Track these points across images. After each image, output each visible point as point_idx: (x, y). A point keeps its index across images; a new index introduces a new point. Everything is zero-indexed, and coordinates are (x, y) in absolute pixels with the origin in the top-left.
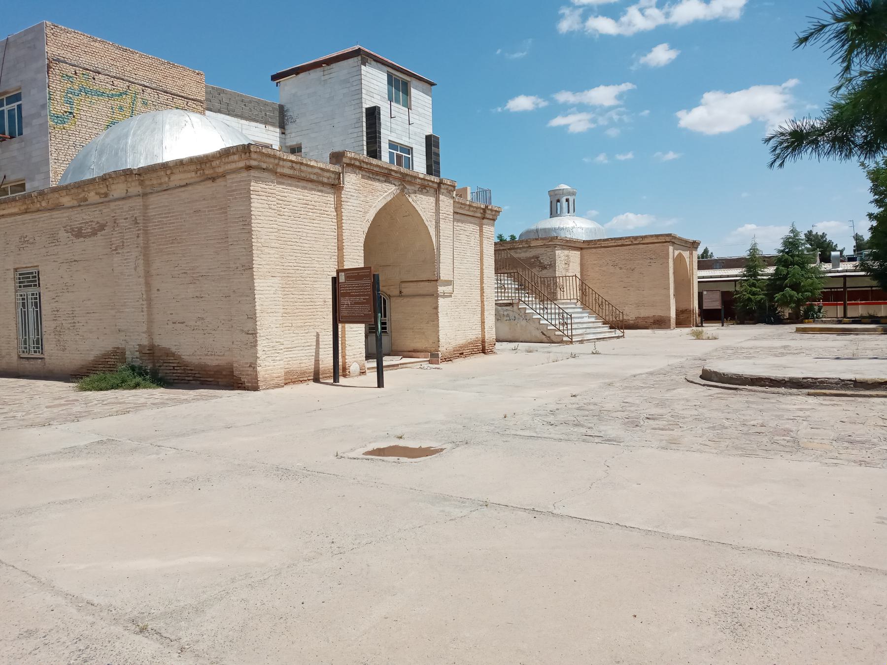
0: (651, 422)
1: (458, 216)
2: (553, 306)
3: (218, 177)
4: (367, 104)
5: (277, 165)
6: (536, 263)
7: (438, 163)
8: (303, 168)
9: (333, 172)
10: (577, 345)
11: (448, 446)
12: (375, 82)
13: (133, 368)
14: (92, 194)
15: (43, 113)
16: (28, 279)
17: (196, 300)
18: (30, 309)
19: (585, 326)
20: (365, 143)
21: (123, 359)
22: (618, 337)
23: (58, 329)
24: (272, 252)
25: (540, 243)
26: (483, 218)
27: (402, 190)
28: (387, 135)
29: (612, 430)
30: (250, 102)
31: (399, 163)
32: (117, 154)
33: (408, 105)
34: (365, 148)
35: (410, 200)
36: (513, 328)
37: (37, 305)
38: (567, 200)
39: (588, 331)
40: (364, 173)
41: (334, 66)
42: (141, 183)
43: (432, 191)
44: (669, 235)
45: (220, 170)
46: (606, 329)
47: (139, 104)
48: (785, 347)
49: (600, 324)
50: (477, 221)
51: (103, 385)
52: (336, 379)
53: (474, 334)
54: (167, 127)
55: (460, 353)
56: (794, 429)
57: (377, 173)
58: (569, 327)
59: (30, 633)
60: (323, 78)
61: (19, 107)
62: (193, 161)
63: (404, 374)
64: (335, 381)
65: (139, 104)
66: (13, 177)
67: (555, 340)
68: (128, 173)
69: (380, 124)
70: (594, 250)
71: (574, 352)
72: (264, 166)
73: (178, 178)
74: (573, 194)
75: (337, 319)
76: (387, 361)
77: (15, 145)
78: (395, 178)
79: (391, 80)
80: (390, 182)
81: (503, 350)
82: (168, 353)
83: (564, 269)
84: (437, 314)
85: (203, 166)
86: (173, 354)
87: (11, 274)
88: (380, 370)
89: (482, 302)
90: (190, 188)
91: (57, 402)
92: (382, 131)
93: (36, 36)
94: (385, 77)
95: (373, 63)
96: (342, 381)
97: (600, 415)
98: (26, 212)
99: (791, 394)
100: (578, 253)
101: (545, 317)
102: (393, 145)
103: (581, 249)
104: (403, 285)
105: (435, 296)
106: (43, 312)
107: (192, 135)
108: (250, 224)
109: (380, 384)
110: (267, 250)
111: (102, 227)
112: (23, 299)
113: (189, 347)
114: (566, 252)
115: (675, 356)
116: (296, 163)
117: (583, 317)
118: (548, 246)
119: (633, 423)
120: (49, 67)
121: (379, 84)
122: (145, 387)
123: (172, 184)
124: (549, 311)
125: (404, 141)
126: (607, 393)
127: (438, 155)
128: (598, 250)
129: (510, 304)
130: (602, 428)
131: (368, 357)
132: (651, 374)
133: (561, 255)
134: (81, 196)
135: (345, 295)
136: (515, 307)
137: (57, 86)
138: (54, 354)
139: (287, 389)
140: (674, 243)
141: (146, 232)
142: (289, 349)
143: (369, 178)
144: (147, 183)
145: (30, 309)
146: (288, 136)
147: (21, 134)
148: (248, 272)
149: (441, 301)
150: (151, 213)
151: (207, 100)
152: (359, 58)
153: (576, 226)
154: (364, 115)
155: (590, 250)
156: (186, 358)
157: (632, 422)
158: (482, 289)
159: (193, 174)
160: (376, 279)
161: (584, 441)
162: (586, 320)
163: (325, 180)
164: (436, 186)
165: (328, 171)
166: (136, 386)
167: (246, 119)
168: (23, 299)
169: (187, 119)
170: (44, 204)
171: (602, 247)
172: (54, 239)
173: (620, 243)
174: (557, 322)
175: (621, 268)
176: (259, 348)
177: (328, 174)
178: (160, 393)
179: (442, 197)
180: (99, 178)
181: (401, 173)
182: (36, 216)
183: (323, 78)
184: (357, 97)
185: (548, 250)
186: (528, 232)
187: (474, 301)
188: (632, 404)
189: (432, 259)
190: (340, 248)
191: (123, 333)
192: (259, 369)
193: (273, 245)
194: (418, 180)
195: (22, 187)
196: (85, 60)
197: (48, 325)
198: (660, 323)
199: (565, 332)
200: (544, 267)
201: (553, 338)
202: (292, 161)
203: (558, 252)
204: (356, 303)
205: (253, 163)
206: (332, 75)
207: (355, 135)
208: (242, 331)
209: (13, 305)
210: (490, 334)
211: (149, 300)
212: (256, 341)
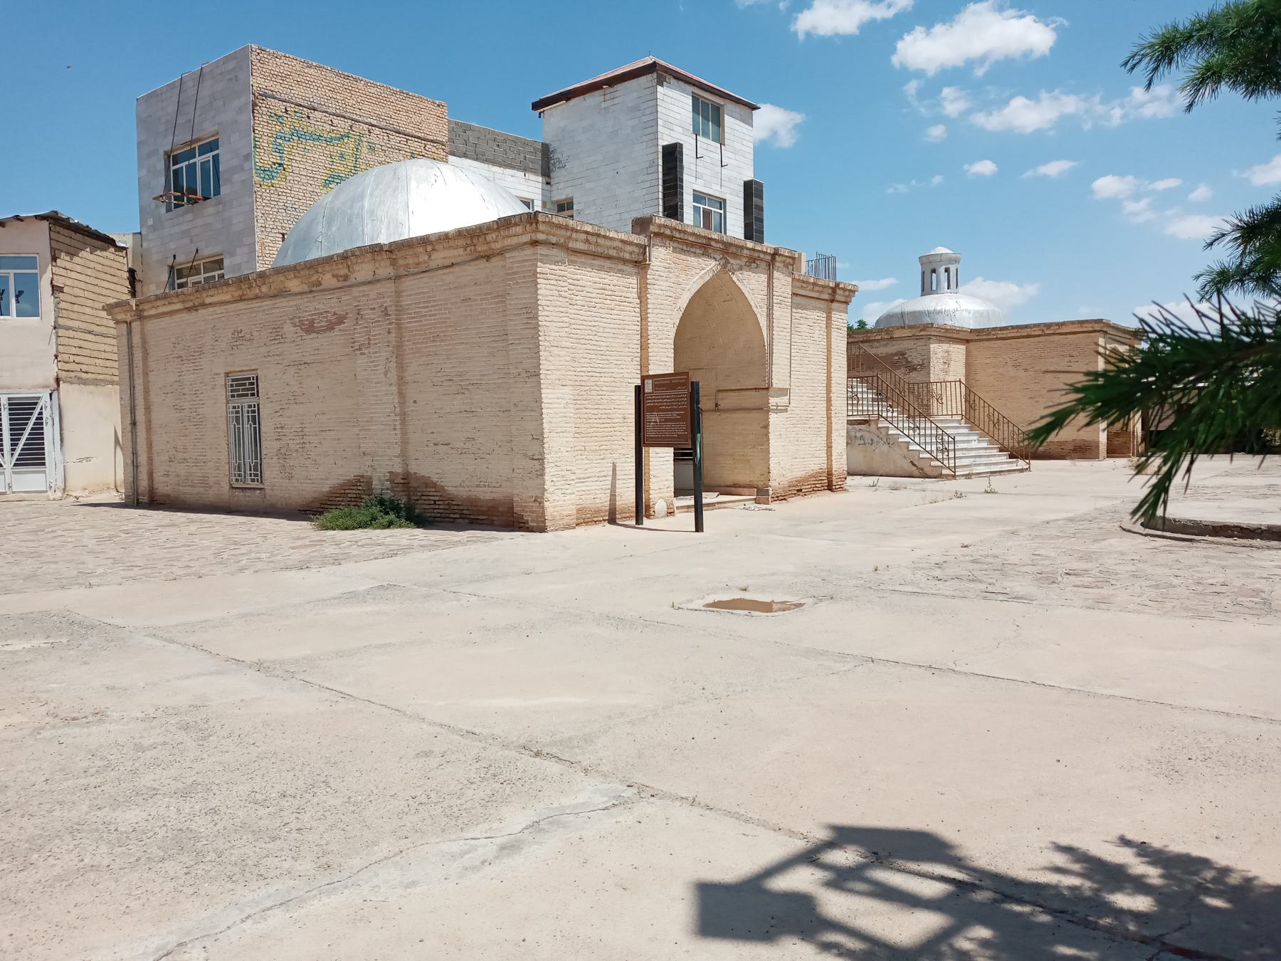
0: (1072, 578)
1: (798, 299)
2: (928, 425)
3: (494, 255)
4: (665, 141)
5: (570, 238)
6: (901, 362)
7: (762, 221)
8: (601, 241)
9: (637, 245)
10: (963, 480)
11: (809, 601)
12: (676, 109)
13: (381, 502)
14: (328, 276)
15: (246, 166)
16: (245, 386)
17: (465, 415)
18: (247, 428)
19: (973, 453)
20: (661, 195)
21: (369, 491)
22: (1022, 470)
23: (283, 451)
24: (562, 353)
25: (907, 333)
26: (832, 301)
27: (725, 266)
28: (690, 183)
29: (1019, 586)
30: (505, 141)
31: (707, 225)
32: (351, 221)
33: (720, 140)
34: (661, 202)
35: (735, 278)
36: (872, 458)
37: (255, 419)
38: (947, 270)
39: (978, 461)
40: (676, 245)
41: (619, 87)
42: (393, 263)
43: (763, 265)
44: (1099, 321)
45: (498, 246)
46: (1004, 458)
47: (365, 150)
48: (1270, 486)
49: (995, 452)
50: (823, 305)
51: (350, 523)
52: (639, 521)
53: (814, 463)
54: (413, 184)
55: (798, 489)
56: (1267, 589)
57: (693, 244)
58: (952, 454)
59: (427, 754)
60: (603, 105)
61: (216, 158)
62: (463, 234)
63: (726, 515)
64: (637, 523)
65: (365, 150)
66: (208, 251)
67: (929, 473)
68: (376, 250)
69: (682, 168)
71: (960, 490)
72: (554, 240)
73: (440, 257)
74: (956, 261)
75: (641, 442)
76: (708, 498)
77: (209, 208)
78: (716, 250)
79: (698, 106)
80: (709, 256)
81: (856, 487)
82: (428, 483)
84: (767, 435)
85: (475, 241)
86: (434, 485)
87: (221, 380)
88: (698, 509)
89: (829, 418)
90: (456, 269)
91: (299, 543)
92: (685, 177)
93: (240, 62)
94: (689, 100)
95: (673, 81)
96: (647, 523)
97: (1003, 569)
98: (241, 300)
99: (1269, 548)
100: (962, 348)
101: (917, 440)
102: (698, 197)
103: (968, 341)
104: (720, 395)
105: (764, 409)
106: (263, 429)
107: (447, 197)
108: (536, 317)
109: (699, 527)
110: (555, 351)
111: (341, 320)
112: (237, 412)
113: (454, 476)
114: (945, 346)
115: (1106, 497)
116: (592, 234)
117: (969, 441)
118: (919, 338)
119: (1048, 579)
120: (254, 105)
121: (681, 111)
122: (400, 527)
123: (433, 264)
124: (922, 432)
125: (714, 190)
126: (1010, 543)
127: (761, 209)
128: (992, 344)
129: (865, 422)
130: (1007, 584)
131: (678, 492)
132: (1071, 520)
133: (938, 350)
134: (314, 278)
135: (652, 409)
136: (873, 426)
137: (265, 129)
138: (276, 483)
139: (580, 531)
140: (1105, 332)
141: (399, 327)
142: (582, 480)
143: (683, 251)
144: (401, 262)
145: (247, 428)
146: (554, 188)
147: (217, 192)
148: (534, 379)
149: (773, 418)
150: (405, 302)
151: (451, 140)
152: (655, 75)
153: (962, 306)
154: (660, 156)
156: (451, 490)
157: (1047, 578)
158: (829, 400)
159: (461, 251)
160: (695, 388)
161: (985, 598)
162: (975, 445)
163: (627, 256)
164: (769, 258)
165: (631, 243)
166: (389, 525)
167: (500, 165)
168: (237, 412)
169: (437, 172)
170: (264, 289)
172: (277, 334)
174: (934, 448)
175: (1026, 370)
176: (547, 477)
177: (629, 248)
178: (420, 533)
179: (776, 274)
180: (338, 255)
181: (723, 243)
182: (255, 304)
183: (603, 105)
184: (649, 131)
185: (919, 343)
186: (889, 317)
187: (817, 417)
188: (1047, 557)
189: (763, 359)
190: (644, 347)
191: (369, 458)
192: (546, 504)
193: (564, 344)
194: (745, 252)
195: (219, 264)
196: (298, 93)
197: (269, 446)
199: (946, 462)
200: (912, 368)
201: (928, 471)
202: (587, 233)
204: (667, 420)
205: (541, 237)
206: (616, 101)
207: (648, 184)
208: (525, 455)
209: (224, 419)
210: (840, 465)
211: (403, 415)
212: (543, 469)
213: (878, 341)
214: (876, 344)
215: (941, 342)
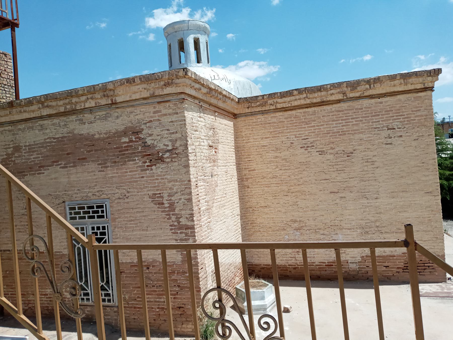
25: (139, 91)
70: (261, 118)
103: (235, 116)
118: (163, 100)
128: (269, 118)
155: (254, 119)
171: (277, 110)
173: (317, 97)
175: (322, 153)
185: (164, 109)
200: (154, 158)
213: (91, 110)
214: (88, 116)
215: (202, 109)
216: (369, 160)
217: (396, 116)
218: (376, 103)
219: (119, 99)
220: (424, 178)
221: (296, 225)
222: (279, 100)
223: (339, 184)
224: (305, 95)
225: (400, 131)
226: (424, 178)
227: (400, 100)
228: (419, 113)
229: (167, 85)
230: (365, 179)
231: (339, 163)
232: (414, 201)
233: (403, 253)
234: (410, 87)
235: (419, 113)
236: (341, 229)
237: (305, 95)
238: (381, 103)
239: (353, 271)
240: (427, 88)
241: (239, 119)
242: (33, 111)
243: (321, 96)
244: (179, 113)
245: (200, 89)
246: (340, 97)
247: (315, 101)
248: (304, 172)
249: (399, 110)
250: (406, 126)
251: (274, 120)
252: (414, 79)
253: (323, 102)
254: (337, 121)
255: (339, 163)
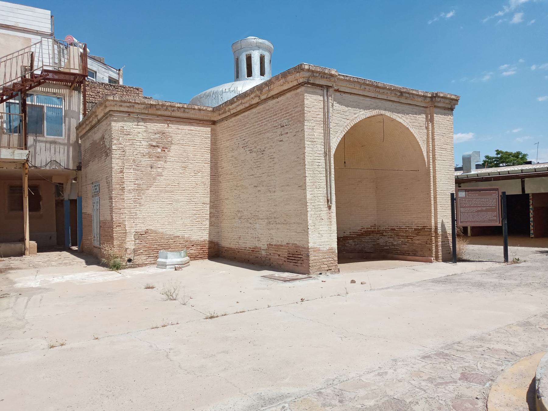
38: (249, 59)
44: (299, 69)
70: (225, 124)
83: (150, 155)
100: (206, 131)
103: (214, 123)
114: (155, 127)
173: (247, 102)
175: (251, 151)
198: (292, 261)
203: (116, 126)
216: (272, 157)
217: (286, 114)
218: (276, 103)
219: (99, 117)
220: (298, 173)
221: (239, 215)
222: (231, 107)
223: (258, 179)
224: (240, 102)
225: (287, 128)
226: (298, 173)
227: (287, 98)
228: (297, 110)
229: (106, 107)
230: (270, 174)
231: (258, 160)
232: (293, 194)
233: (287, 244)
234: (291, 85)
235: (297, 110)
236: (258, 219)
237: (240, 102)
238: (278, 102)
239: (264, 257)
240: (299, 84)
241: (218, 125)
242: (85, 128)
243: (249, 101)
244: (110, 124)
245: (133, 106)
246: (256, 100)
247: (247, 105)
248: (243, 169)
249: (287, 107)
250: (290, 123)
251: (232, 124)
252: (290, 77)
253: (252, 105)
254: (258, 122)
255: (258, 160)
